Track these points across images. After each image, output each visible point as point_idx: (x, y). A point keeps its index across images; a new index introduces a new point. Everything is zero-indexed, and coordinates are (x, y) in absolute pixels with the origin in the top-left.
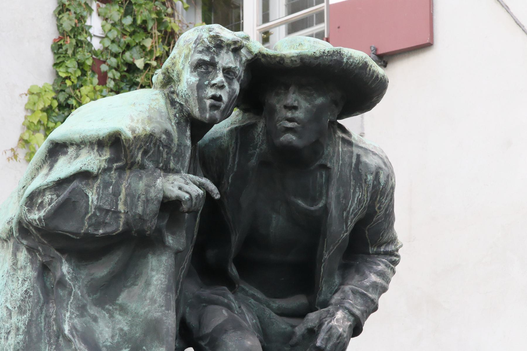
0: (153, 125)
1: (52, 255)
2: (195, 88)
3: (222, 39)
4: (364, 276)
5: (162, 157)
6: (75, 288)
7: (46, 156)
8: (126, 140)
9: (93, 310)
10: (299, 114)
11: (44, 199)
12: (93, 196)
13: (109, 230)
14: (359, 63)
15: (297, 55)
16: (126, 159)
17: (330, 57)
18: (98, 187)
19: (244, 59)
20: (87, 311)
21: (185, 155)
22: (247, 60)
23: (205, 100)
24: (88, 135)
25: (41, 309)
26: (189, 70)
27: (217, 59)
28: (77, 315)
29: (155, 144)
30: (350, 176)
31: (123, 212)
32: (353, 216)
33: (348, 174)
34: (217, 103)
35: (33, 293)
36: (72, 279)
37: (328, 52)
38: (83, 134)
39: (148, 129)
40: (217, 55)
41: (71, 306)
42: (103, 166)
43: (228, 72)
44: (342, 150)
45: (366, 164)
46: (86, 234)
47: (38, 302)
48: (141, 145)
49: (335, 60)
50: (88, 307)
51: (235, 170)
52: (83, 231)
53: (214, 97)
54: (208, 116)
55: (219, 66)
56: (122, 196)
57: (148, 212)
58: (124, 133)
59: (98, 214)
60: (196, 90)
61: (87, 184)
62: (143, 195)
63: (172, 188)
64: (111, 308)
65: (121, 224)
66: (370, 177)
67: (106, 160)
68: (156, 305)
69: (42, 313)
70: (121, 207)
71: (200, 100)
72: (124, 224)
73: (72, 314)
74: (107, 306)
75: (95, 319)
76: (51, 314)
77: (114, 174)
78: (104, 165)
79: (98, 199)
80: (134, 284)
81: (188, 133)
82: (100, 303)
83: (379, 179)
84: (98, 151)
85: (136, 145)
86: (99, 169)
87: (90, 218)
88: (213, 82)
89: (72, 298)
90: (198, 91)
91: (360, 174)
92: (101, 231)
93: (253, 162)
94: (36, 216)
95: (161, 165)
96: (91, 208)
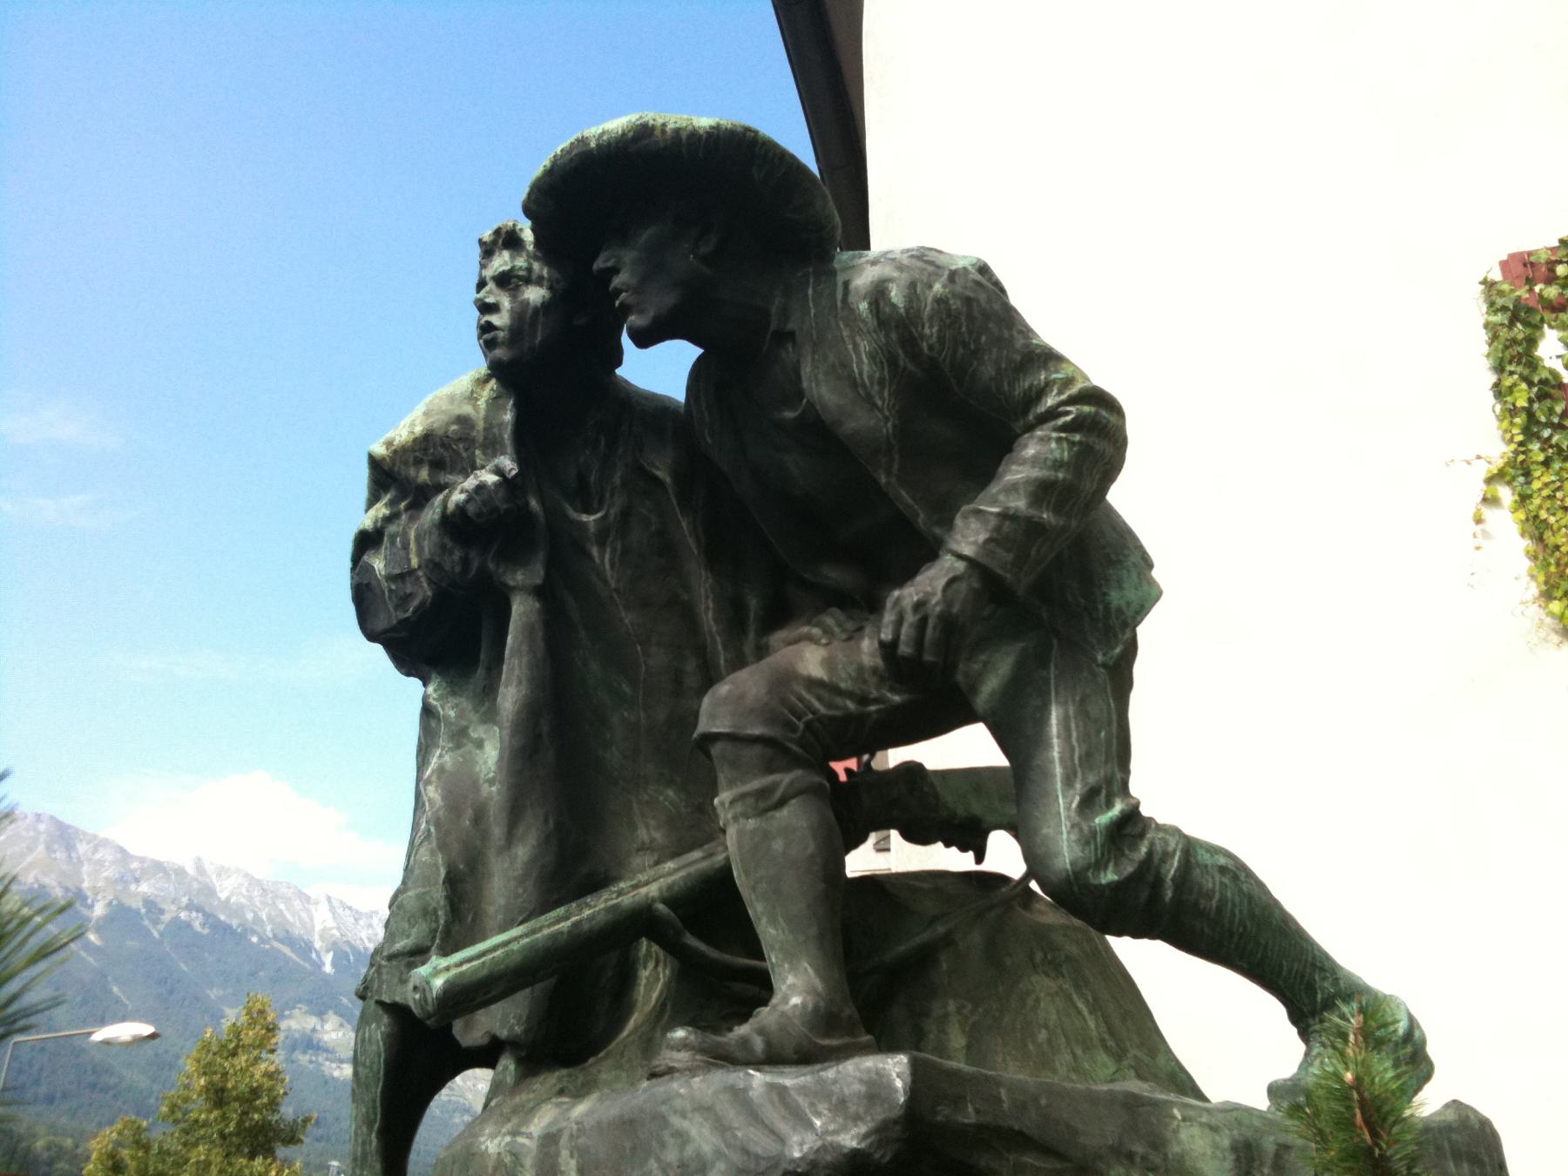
0: (430, 420)
6: (443, 709)
18: (386, 548)
21: (503, 438)
28: (450, 748)
29: (443, 445)
32: (876, 388)
49: (576, 155)
55: (488, 279)
67: (386, 504)
72: (429, 585)
83: (890, 299)
87: (390, 598)
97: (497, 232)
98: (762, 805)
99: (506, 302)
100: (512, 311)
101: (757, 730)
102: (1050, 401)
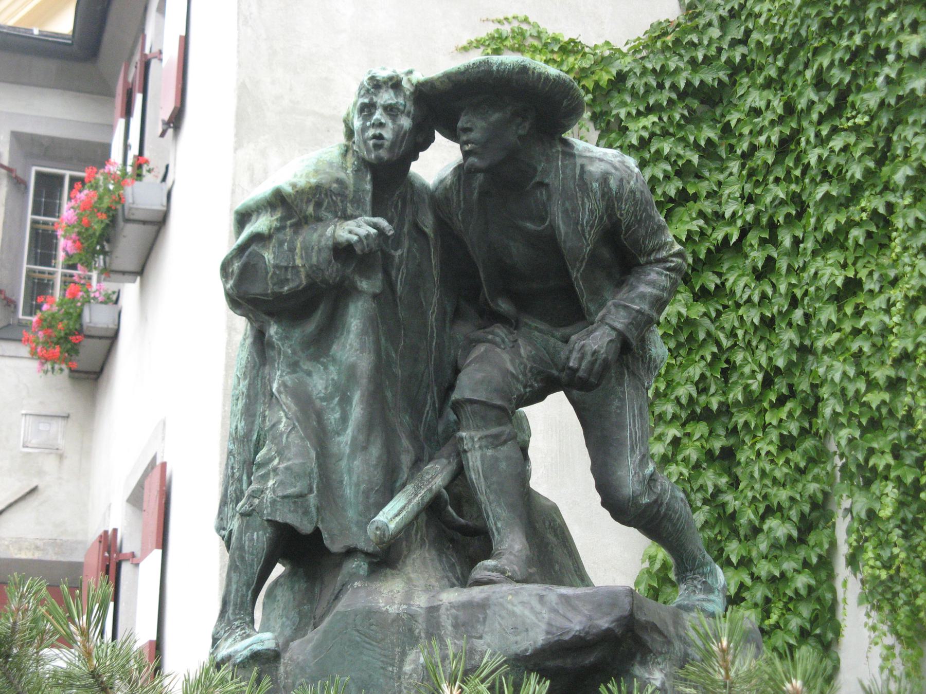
0: (320, 177)
3: (378, 78)
4: (633, 288)
9: (306, 365)
10: (474, 135)
12: (269, 256)
13: (292, 285)
14: (513, 68)
17: (477, 69)
18: (274, 246)
19: (408, 93)
20: (300, 367)
22: (412, 93)
25: (258, 372)
27: (375, 99)
29: (326, 195)
30: (575, 188)
32: (589, 228)
33: (572, 187)
34: (380, 142)
36: (280, 339)
37: (474, 64)
39: (313, 181)
40: (376, 95)
42: (274, 226)
43: (390, 110)
45: (590, 172)
46: (273, 293)
47: (254, 366)
48: (308, 198)
49: (482, 71)
50: (301, 364)
51: (462, 206)
52: (269, 291)
53: (375, 137)
54: (373, 156)
55: (378, 105)
56: (298, 251)
59: (278, 273)
61: (264, 246)
63: (342, 234)
64: (325, 360)
66: (595, 185)
70: (299, 262)
72: (306, 277)
73: (283, 371)
75: (309, 374)
77: (288, 231)
78: (275, 224)
80: (342, 334)
81: (369, 177)
82: (315, 358)
83: (609, 185)
84: (271, 212)
85: (302, 200)
86: (270, 229)
87: (272, 277)
91: (586, 184)
92: (286, 288)
93: (476, 194)
97: (391, 78)
98: (496, 442)
99: (390, 124)
100: (393, 129)
101: (499, 402)
102: (664, 254)
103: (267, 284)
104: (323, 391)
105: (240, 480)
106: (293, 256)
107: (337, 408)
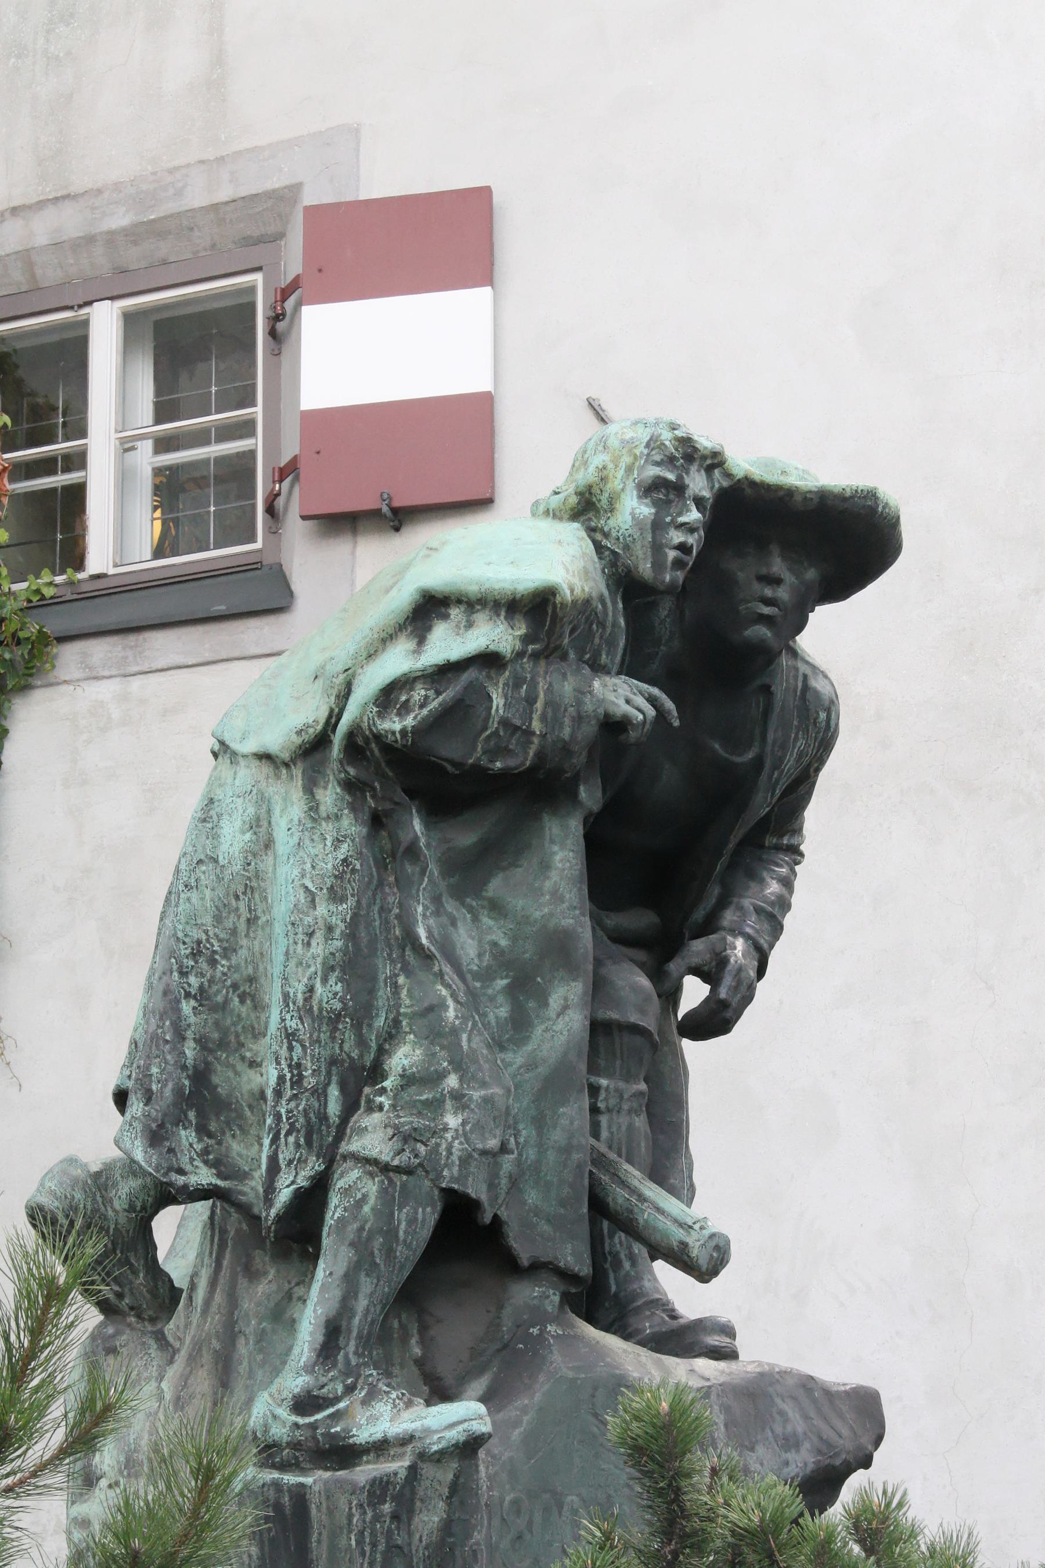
1: (397, 799)
2: (649, 526)
3: (698, 446)
5: (593, 641)
7: (408, 617)
8: (562, 604)
9: (450, 905)
10: (783, 593)
11: (412, 696)
13: (512, 762)
15: (816, 490)
16: (549, 639)
23: (667, 550)
24: (497, 587)
25: (374, 895)
26: (635, 493)
27: (687, 481)
31: (538, 733)
33: (792, 706)
35: (361, 865)
37: (862, 490)
38: (487, 586)
41: (423, 895)
44: (787, 665)
45: (817, 693)
47: (370, 883)
49: (869, 506)
50: (444, 899)
52: (471, 761)
54: (668, 578)
55: (689, 493)
56: (539, 705)
57: (579, 739)
58: (562, 592)
59: (502, 733)
60: (650, 531)
62: (572, 706)
63: (615, 700)
64: (474, 904)
65: (531, 754)
67: (521, 636)
68: (565, 905)
69: (374, 903)
70: (536, 726)
71: (657, 548)
72: (535, 755)
74: (468, 900)
76: (390, 906)
79: (505, 705)
80: (514, 865)
82: (459, 894)
84: (506, 618)
87: (489, 737)
88: (682, 519)
89: (426, 879)
90: (654, 532)
91: (808, 710)
92: (498, 764)
94: (394, 725)
95: (587, 656)
96: (493, 723)
103: (474, 748)
104: (476, 961)
105: (320, 1093)
106: (531, 713)
107: (501, 999)
